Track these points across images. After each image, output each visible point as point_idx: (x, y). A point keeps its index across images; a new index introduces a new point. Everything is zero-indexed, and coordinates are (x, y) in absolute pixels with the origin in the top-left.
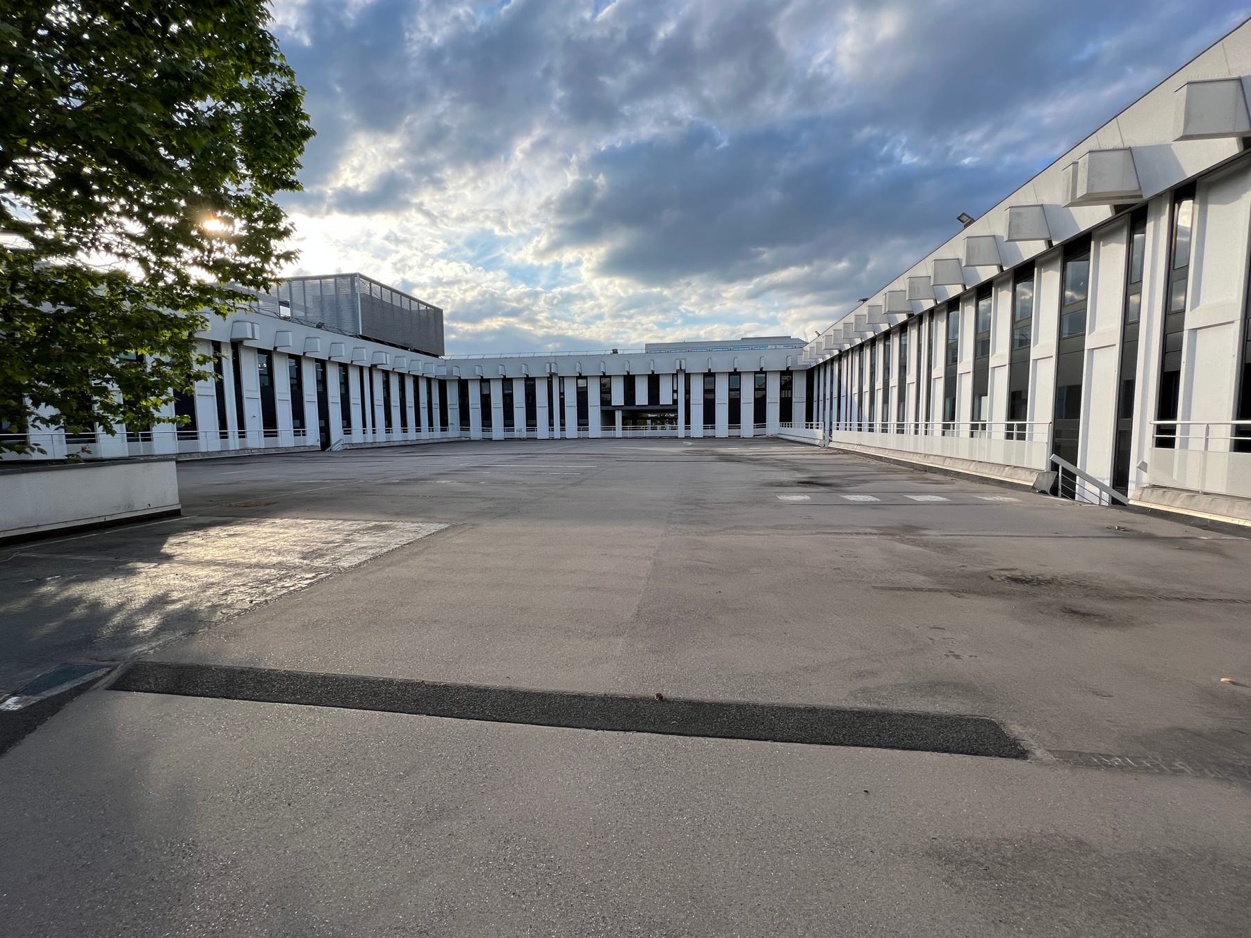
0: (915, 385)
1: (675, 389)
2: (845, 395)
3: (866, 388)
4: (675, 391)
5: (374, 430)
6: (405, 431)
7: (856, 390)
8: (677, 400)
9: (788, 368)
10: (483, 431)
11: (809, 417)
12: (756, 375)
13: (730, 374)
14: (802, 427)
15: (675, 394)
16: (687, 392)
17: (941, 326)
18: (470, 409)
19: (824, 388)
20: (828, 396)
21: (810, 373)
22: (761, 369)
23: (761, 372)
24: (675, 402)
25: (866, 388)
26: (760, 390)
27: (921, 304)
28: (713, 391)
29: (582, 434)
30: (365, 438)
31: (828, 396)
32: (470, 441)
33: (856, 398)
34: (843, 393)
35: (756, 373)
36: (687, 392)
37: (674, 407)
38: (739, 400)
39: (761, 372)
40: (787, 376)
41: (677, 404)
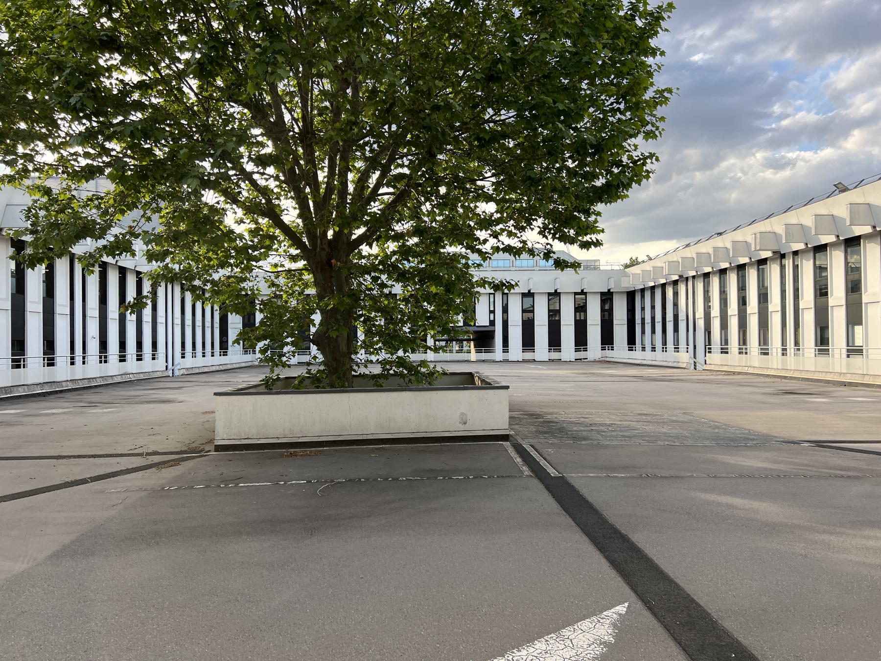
0: (779, 314)
1: (492, 309)
2: (685, 318)
3: (715, 311)
4: (492, 312)
5: (184, 354)
6: (51, 363)
7: (700, 313)
8: (494, 321)
9: (609, 290)
10: (603, 349)
11: (631, 341)
12: (576, 296)
13: (549, 294)
14: (623, 350)
15: (492, 318)
16: (505, 310)
17: (807, 267)
18: (229, 330)
19: (645, 310)
20: (648, 319)
21: (631, 296)
22: (582, 291)
23: (583, 293)
24: (492, 323)
25: (715, 311)
26: (581, 308)
27: (790, 245)
28: (558, 312)
29: (555, 355)
30: (73, 373)
31: (648, 319)
32: (494, 361)
33: (701, 323)
34: (682, 316)
35: (576, 294)
36: (505, 310)
37: (491, 328)
38: (585, 321)
39: (583, 293)
40: (607, 298)
41: (494, 325)
